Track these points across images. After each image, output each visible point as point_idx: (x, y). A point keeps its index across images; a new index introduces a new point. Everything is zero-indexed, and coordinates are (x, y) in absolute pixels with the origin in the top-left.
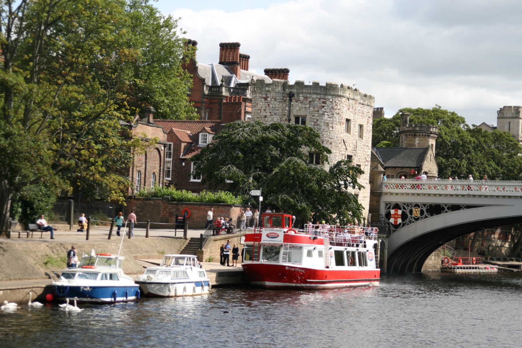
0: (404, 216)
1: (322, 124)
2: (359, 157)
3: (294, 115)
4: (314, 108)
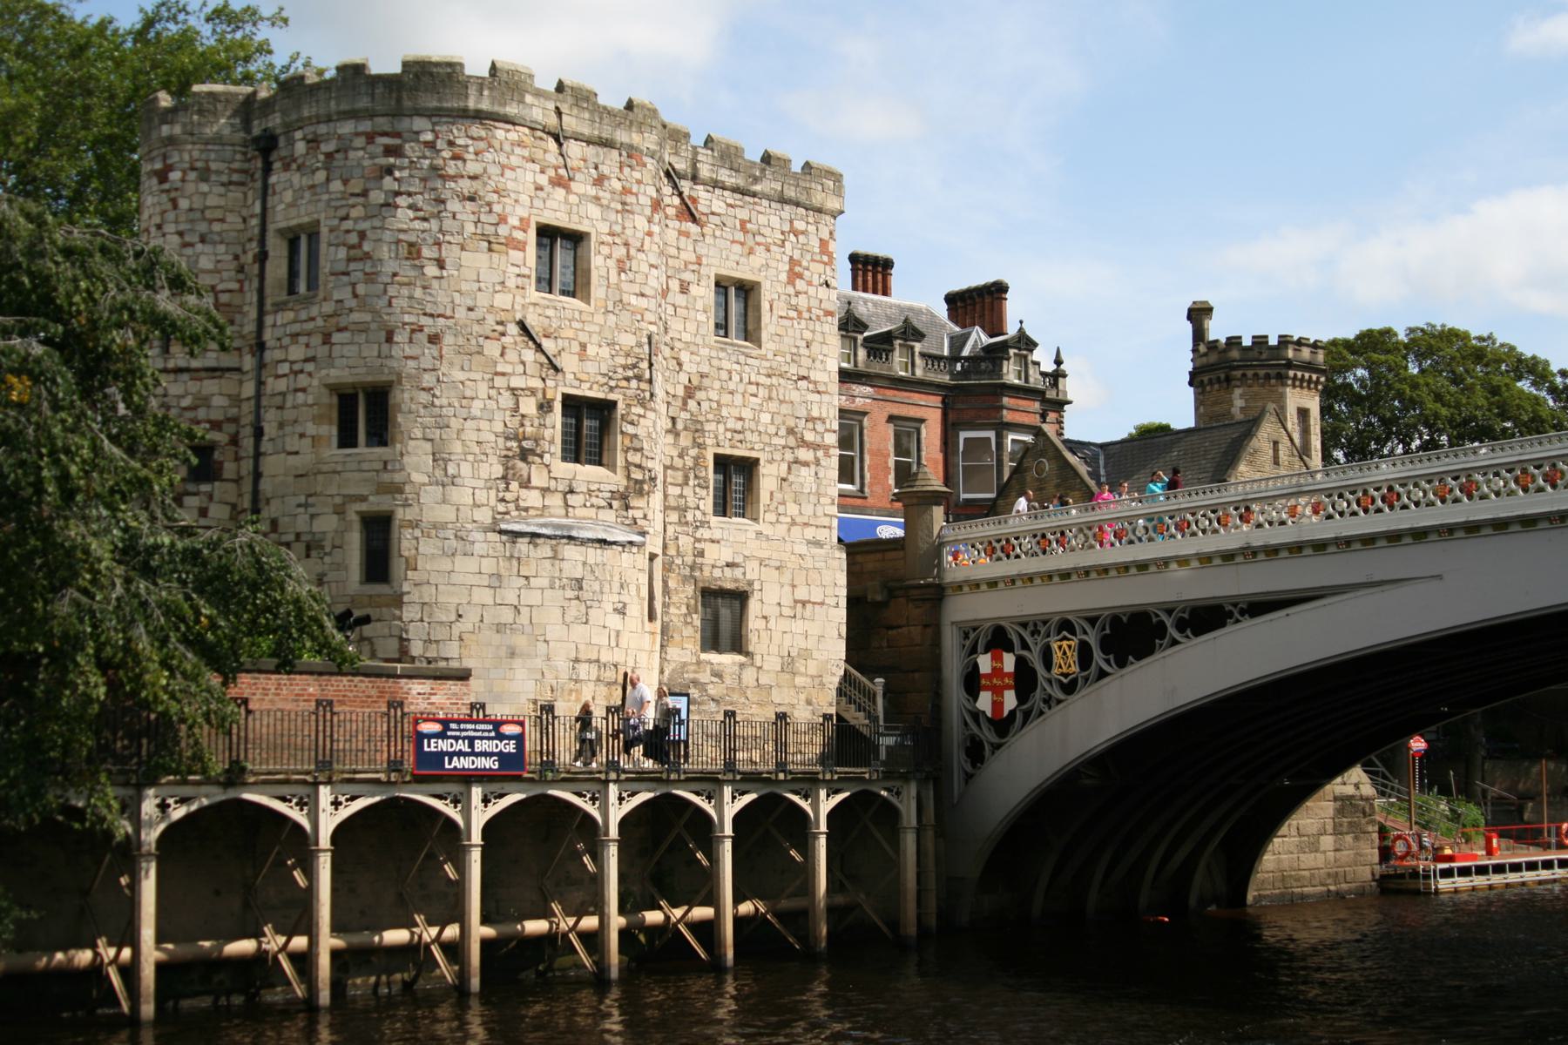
0: (1024, 680)
1: (384, 252)
3: (281, 232)
4: (345, 182)
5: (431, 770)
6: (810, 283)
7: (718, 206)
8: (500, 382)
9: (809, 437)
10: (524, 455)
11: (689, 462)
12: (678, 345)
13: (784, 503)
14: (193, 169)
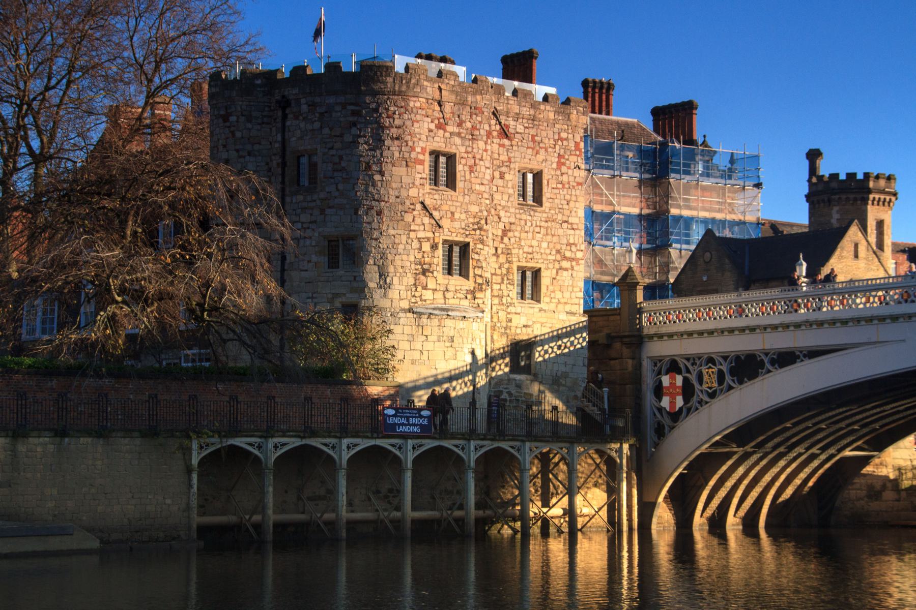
0: (688, 390)
4: (331, 129)
5: (389, 431)
6: (569, 168)
7: (520, 128)
8: (412, 235)
9: (568, 254)
10: (424, 272)
11: (504, 271)
12: (499, 208)
13: (554, 292)
14: (243, 115)
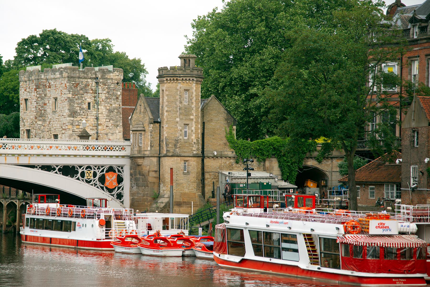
2: (55, 128)
9: (64, 128)
